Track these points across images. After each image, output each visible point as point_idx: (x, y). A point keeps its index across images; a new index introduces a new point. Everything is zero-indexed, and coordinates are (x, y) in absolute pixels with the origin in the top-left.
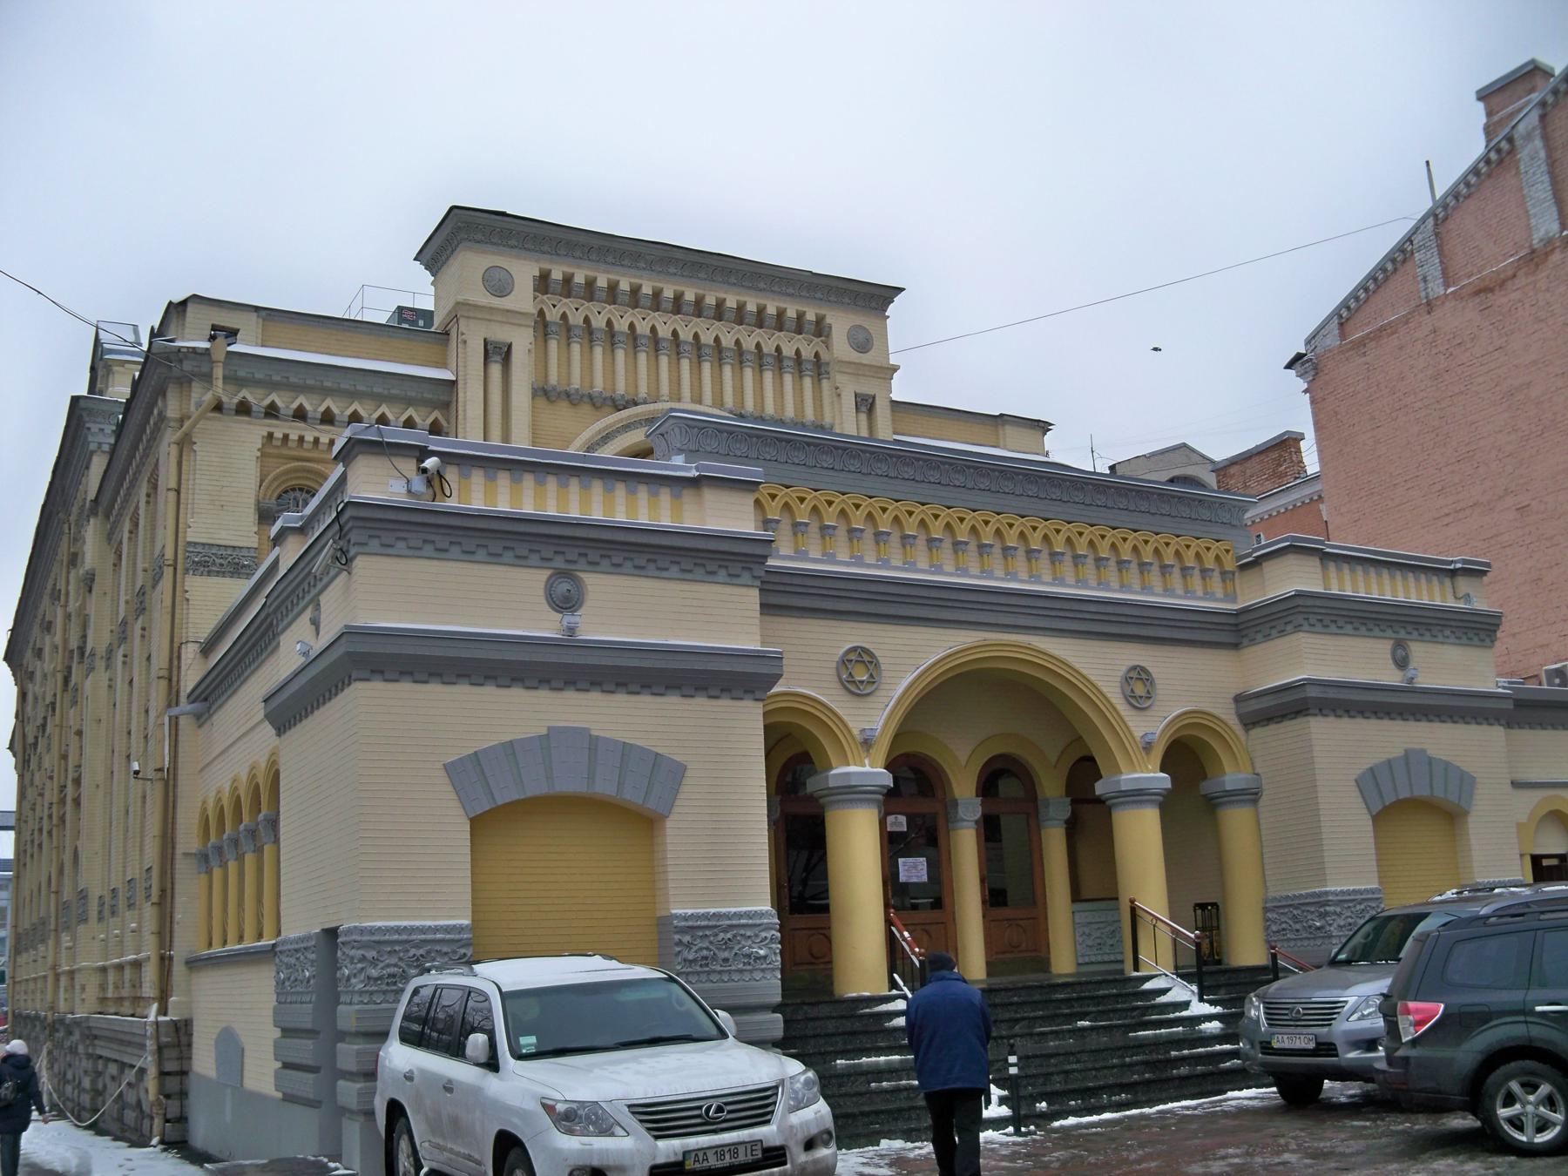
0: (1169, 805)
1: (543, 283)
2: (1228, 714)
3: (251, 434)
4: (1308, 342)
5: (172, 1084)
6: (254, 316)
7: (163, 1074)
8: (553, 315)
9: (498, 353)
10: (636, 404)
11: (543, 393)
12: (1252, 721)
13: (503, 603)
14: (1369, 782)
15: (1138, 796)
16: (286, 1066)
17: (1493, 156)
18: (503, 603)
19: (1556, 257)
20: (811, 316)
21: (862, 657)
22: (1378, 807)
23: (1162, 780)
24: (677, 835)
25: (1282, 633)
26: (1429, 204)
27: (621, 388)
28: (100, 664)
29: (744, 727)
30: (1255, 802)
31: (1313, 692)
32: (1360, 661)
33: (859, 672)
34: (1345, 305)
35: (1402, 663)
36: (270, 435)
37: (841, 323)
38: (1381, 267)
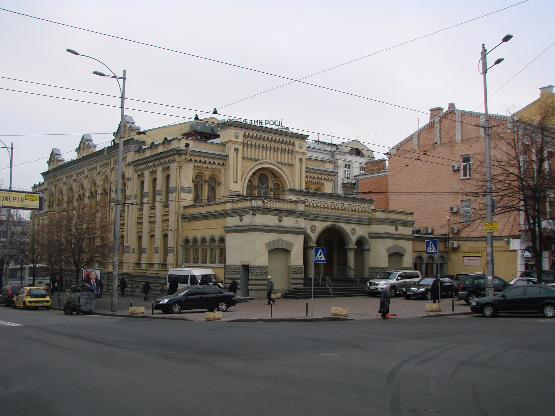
1: (244, 135)
2: (367, 236)
8: (245, 142)
9: (236, 150)
10: (259, 160)
12: (371, 238)
13: (271, 220)
15: (352, 249)
20: (292, 142)
21: (314, 226)
23: (355, 247)
24: (293, 254)
26: (417, 129)
27: (257, 157)
28: (133, 198)
29: (301, 238)
32: (390, 229)
33: (313, 228)
37: (297, 143)
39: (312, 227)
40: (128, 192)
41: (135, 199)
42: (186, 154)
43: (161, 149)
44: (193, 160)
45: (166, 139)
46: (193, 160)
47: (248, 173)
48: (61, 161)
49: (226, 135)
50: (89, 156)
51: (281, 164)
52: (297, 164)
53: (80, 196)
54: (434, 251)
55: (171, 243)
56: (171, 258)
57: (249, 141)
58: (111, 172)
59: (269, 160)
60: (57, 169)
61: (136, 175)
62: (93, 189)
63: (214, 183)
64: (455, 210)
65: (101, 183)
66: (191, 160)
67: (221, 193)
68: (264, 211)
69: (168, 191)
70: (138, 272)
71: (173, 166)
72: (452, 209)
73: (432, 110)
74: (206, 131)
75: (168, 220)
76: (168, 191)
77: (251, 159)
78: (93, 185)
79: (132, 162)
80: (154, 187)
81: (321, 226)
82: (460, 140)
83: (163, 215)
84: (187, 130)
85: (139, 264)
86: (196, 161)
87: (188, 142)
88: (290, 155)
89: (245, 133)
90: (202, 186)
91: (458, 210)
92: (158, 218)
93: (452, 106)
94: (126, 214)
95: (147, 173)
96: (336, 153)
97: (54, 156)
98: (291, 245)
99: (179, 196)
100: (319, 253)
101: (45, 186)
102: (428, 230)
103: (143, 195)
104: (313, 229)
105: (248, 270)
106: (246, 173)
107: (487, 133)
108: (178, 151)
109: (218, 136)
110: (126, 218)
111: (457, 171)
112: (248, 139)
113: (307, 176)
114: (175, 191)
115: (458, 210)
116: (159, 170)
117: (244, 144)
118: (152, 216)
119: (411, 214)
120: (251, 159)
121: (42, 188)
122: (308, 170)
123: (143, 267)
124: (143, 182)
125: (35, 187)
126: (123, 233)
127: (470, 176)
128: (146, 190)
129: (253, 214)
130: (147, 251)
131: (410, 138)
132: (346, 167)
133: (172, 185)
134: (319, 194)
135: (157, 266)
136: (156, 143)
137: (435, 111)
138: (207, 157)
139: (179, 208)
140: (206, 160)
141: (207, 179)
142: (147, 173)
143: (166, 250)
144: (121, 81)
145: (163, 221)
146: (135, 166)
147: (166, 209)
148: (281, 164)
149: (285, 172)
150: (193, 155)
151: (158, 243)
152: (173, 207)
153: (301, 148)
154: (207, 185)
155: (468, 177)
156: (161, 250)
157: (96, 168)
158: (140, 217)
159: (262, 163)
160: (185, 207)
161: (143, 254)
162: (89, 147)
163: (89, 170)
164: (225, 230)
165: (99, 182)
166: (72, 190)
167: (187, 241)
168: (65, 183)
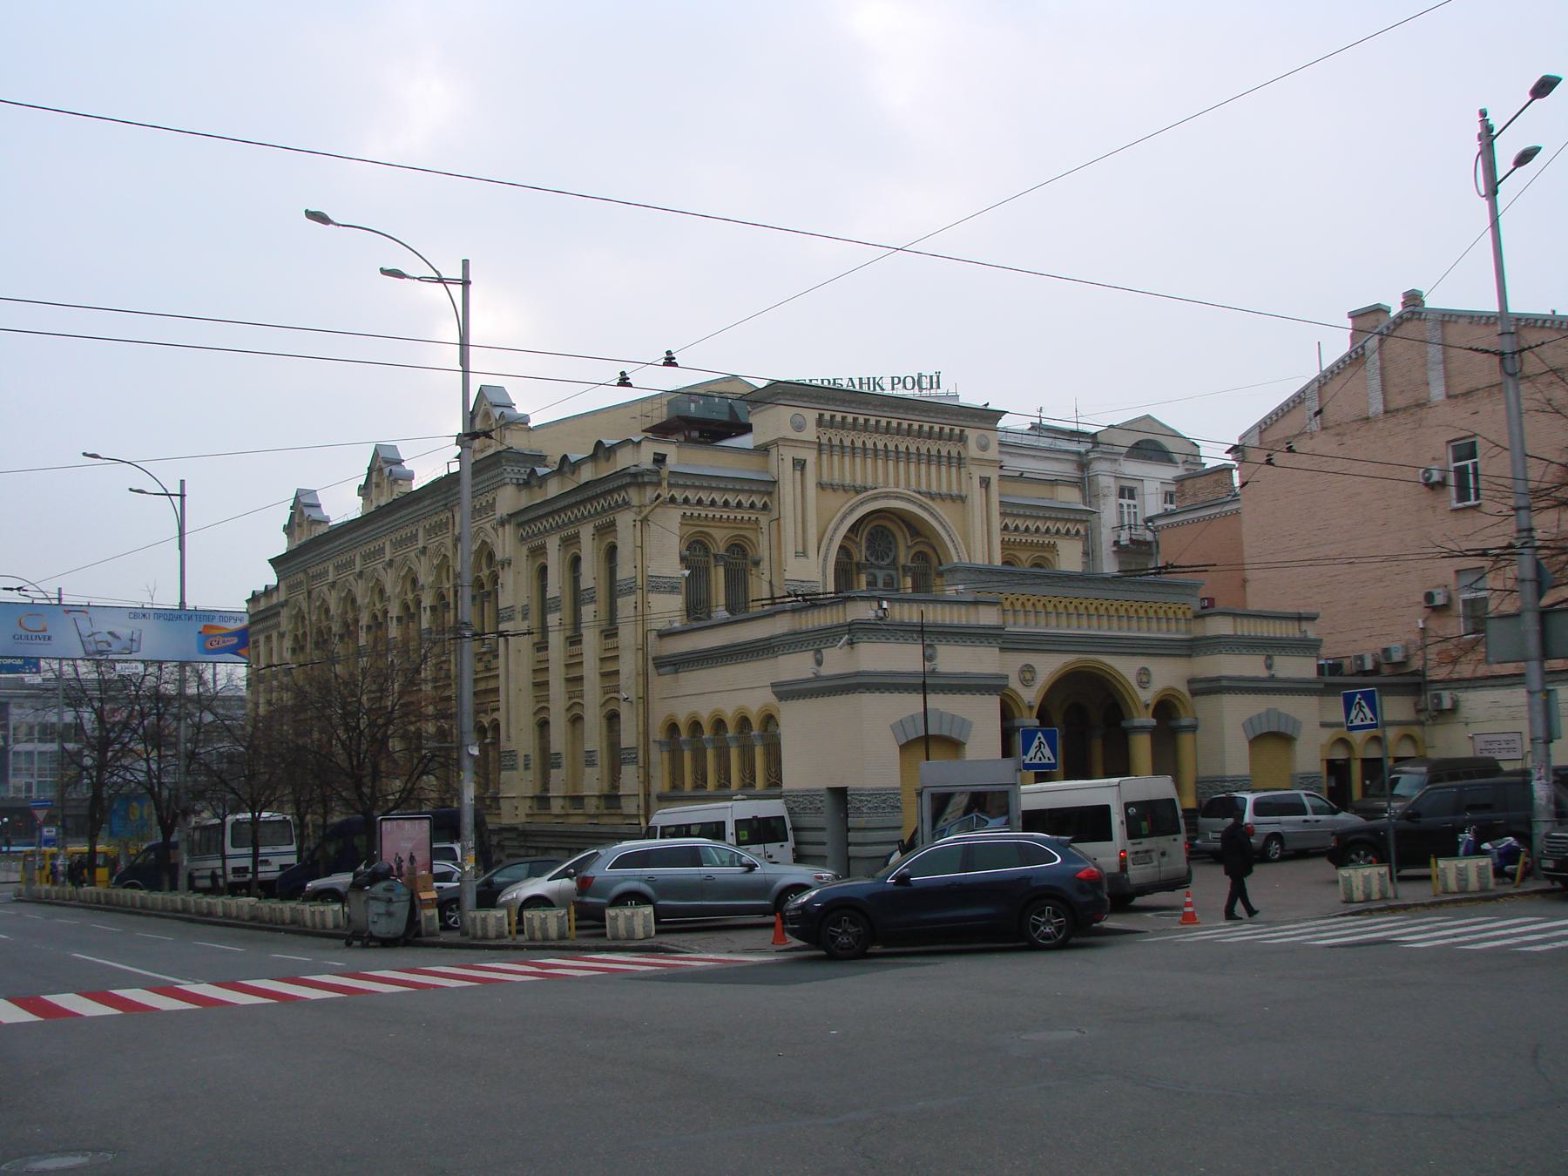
0: (1154, 733)
1: (820, 422)
2: (1183, 688)
3: (674, 515)
4: (1241, 439)
8: (824, 440)
9: (800, 465)
10: (866, 489)
11: (821, 486)
12: (1194, 693)
13: (904, 658)
14: (1249, 724)
15: (1142, 729)
18: (904, 658)
19: (1380, 425)
23: (1153, 722)
26: (1316, 373)
27: (859, 482)
28: (519, 617)
29: (993, 704)
31: (1225, 683)
32: (1249, 666)
33: (1027, 674)
34: (1264, 421)
35: (1269, 667)
38: (1286, 404)
39: (1022, 671)
40: (505, 601)
41: (525, 617)
42: (659, 484)
43: (587, 474)
44: (680, 498)
45: (599, 443)
46: (680, 498)
47: (836, 530)
48: (319, 522)
49: (768, 424)
50: (393, 500)
51: (930, 496)
52: (976, 495)
53: (375, 617)
54: (1368, 722)
55: (628, 737)
56: (630, 779)
57: (835, 436)
58: (455, 546)
59: (897, 485)
60: (311, 545)
61: (524, 550)
62: (410, 596)
63: (740, 561)
64: (1439, 600)
65: (431, 579)
66: (673, 500)
67: (759, 588)
68: (881, 629)
69: (614, 590)
70: (543, 822)
71: (625, 520)
72: (1429, 597)
73: (1354, 316)
74: (715, 416)
75: (617, 672)
76: (614, 590)
77: (845, 489)
78: (408, 584)
79: (511, 516)
80: (576, 580)
81: (1049, 666)
82: (1442, 397)
83: (602, 660)
84: (660, 415)
85: (542, 800)
86: (686, 501)
87: (662, 449)
88: (954, 470)
89: (821, 415)
90: (707, 569)
91: (1449, 598)
92: (591, 669)
93: (1413, 299)
94: (502, 659)
95: (553, 544)
96: (1092, 456)
97: (303, 509)
98: (965, 725)
99: (645, 603)
100: (1036, 742)
101: (281, 597)
102: (1363, 664)
103: (545, 607)
104: (1028, 676)
106: (832, 526)
107: (1510, 370)
108: (635, 475)
109: (746, 429)
110: (501, 671)
111: (1437, 487)
112: (831, 433)
113: (1006, 528)
114: (631, 591)
115: (1449, 598)
116: (587, 532)
117: (820, 445)
118: (574, 663)
119: (1312, 618)
120: (845, 489)
121: (274, 600)
122: (1008, 509)
123: (556, 807)
124: (543, 570)
125: (255, 598)
126: (495, 715)
127: (1477, 498)
128: (553, 590)
129: (851, 643)
130: (564, 762)
131: (1298, 399)
132: (1122, 496)
133: (624, 572)
134: (1043, 574)
135: (594, 802)
136: (573, 458)
137: (1367, 320)
138: (718, 489)
140: (717, 496)
141: (722, 552)
142: (553, 544)
143: (617, 757)
144: (457, 290)
145: (604, 675)
146: (519, 525)
147: (610, 643)
148: (930, 496)
149: (941, 519)
150: (677, 485)
151: (594, 736)
152: (628, 635)
153: (984, 448)
154: (722, 568)
155: (1472, 502)
156: (602, 759)
157: (415, 537)
158: (541, 669)
159: (875, 498)
160: (663, 635)
161: (553, 771)
162: (395, 480)
163: (397, 544)
165: (425, 577)
166: (354, 601)
167: (673, 728)
168: (333, 585)
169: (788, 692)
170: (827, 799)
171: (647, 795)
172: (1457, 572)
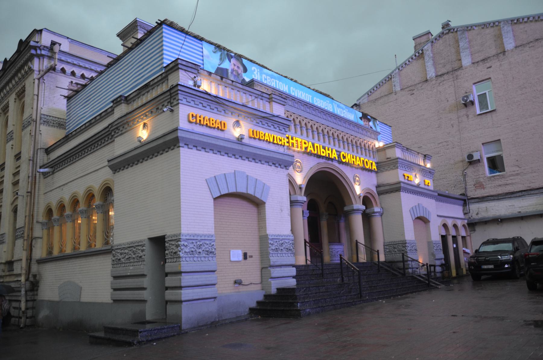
2: (374, 190)
5: (30, 304)
6: (66, 40)
7: (27, 301)
12: (380, 193)
15: (358, 210)
16: (115, 290)
17: (417, 54)
19: (434, 82)
22: (414, 218)
24: (270, 210)
25: (392, 169)
30: (381, 215)
36: (72, 82)
64: (476, 157)
72: (470, 156)
105: (164, 249)
139: (35, 152)
164: (111, 167)
167: (49, 212)
169: (119, 165)
170: (148, 248)
171: (29, 259)
172: (483, 144)
